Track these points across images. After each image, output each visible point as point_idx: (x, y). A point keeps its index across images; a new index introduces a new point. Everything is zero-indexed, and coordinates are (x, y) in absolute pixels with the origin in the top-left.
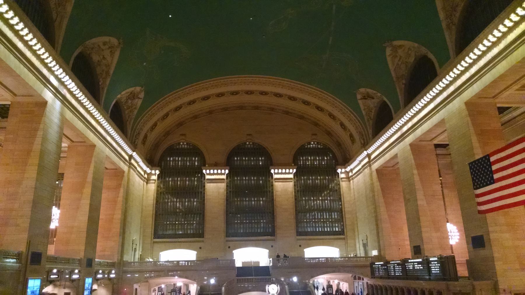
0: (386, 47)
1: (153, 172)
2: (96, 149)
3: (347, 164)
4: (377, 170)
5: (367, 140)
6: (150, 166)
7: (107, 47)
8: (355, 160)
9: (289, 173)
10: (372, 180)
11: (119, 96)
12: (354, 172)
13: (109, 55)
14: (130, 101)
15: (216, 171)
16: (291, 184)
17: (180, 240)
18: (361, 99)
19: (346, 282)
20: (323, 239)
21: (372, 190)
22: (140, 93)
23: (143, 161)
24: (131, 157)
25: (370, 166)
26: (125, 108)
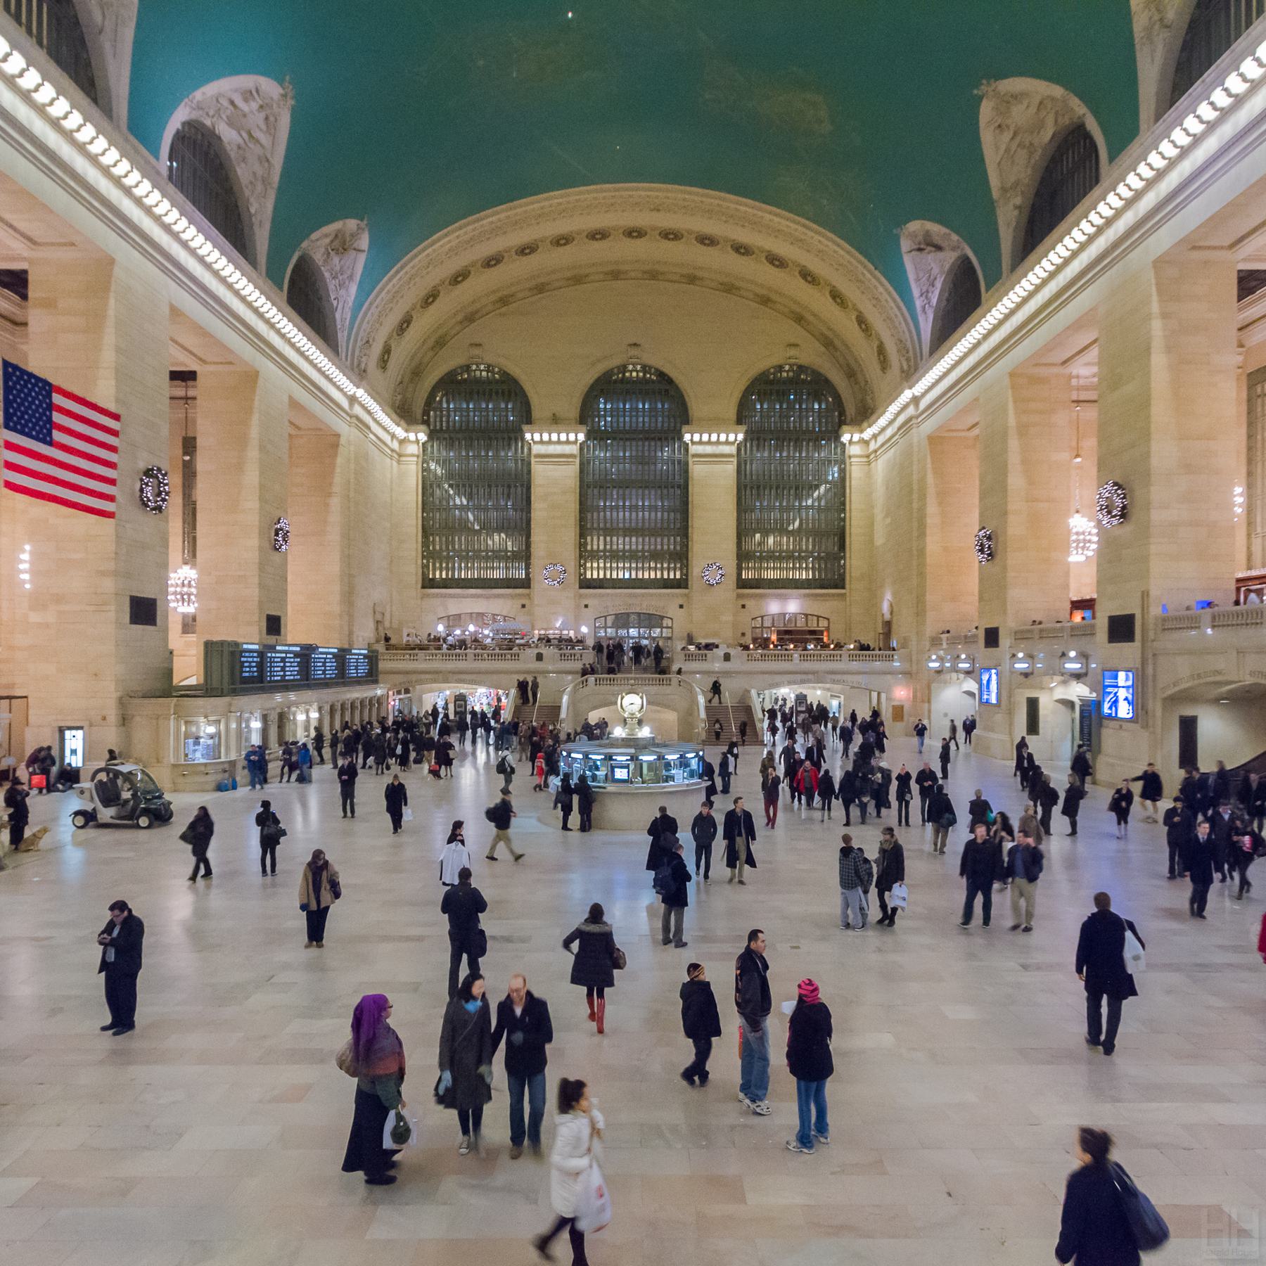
0: (981, 98)
1: (412, 436)
2: (261, 382)
3: (865, 424)
5: (916, 362)
6: (402, 422)
9: (727, 443)
11: (304, 245)
12: (881, 439)
13: (264, 127)
14: (336, 260)
15: (554, 437)
16: (729, 469)
23: (383, 410)
24: (353, 399)
26: (327, 275)
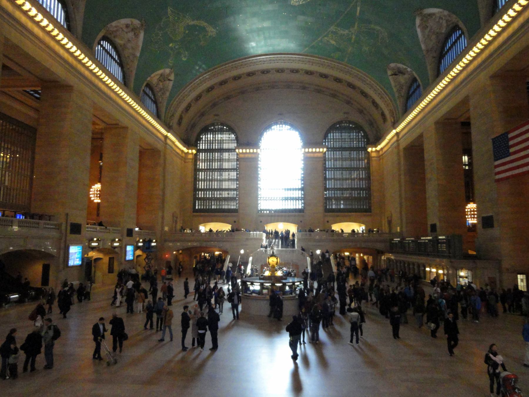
1: (190, 151)
3: (377, 144)
4: (405, 149)
7: (130, 29)
8: (385, 139)
10: (399, 159)
11: (148, 79)
14: (161, 84)
17: (216, 214)
18: (392, 75)
19: (370, 255)
20: (350, 216)
21: (399, 170)
22: (169, 75)
23: (179, 141)
24: (166, 137)
25: (398, 145)
